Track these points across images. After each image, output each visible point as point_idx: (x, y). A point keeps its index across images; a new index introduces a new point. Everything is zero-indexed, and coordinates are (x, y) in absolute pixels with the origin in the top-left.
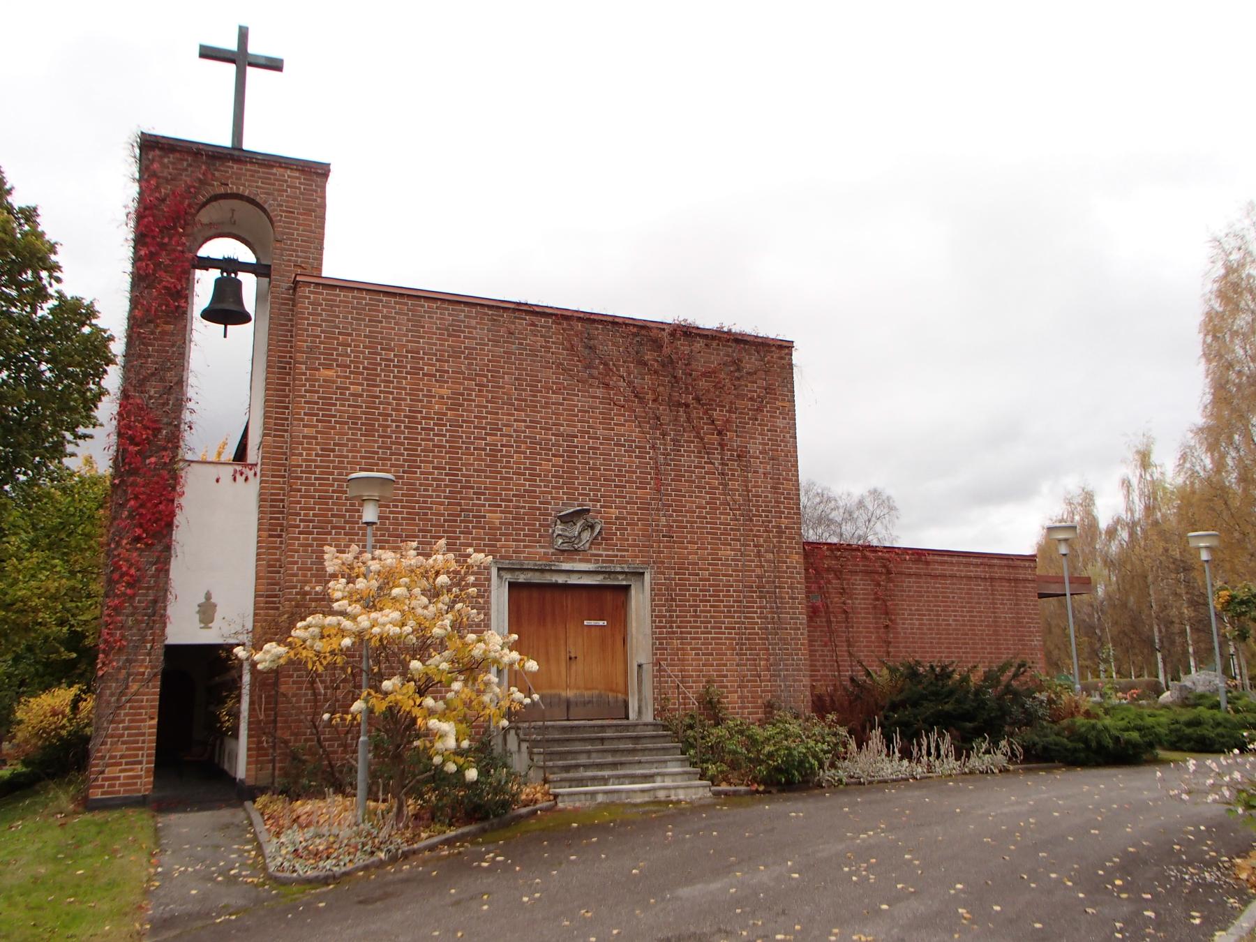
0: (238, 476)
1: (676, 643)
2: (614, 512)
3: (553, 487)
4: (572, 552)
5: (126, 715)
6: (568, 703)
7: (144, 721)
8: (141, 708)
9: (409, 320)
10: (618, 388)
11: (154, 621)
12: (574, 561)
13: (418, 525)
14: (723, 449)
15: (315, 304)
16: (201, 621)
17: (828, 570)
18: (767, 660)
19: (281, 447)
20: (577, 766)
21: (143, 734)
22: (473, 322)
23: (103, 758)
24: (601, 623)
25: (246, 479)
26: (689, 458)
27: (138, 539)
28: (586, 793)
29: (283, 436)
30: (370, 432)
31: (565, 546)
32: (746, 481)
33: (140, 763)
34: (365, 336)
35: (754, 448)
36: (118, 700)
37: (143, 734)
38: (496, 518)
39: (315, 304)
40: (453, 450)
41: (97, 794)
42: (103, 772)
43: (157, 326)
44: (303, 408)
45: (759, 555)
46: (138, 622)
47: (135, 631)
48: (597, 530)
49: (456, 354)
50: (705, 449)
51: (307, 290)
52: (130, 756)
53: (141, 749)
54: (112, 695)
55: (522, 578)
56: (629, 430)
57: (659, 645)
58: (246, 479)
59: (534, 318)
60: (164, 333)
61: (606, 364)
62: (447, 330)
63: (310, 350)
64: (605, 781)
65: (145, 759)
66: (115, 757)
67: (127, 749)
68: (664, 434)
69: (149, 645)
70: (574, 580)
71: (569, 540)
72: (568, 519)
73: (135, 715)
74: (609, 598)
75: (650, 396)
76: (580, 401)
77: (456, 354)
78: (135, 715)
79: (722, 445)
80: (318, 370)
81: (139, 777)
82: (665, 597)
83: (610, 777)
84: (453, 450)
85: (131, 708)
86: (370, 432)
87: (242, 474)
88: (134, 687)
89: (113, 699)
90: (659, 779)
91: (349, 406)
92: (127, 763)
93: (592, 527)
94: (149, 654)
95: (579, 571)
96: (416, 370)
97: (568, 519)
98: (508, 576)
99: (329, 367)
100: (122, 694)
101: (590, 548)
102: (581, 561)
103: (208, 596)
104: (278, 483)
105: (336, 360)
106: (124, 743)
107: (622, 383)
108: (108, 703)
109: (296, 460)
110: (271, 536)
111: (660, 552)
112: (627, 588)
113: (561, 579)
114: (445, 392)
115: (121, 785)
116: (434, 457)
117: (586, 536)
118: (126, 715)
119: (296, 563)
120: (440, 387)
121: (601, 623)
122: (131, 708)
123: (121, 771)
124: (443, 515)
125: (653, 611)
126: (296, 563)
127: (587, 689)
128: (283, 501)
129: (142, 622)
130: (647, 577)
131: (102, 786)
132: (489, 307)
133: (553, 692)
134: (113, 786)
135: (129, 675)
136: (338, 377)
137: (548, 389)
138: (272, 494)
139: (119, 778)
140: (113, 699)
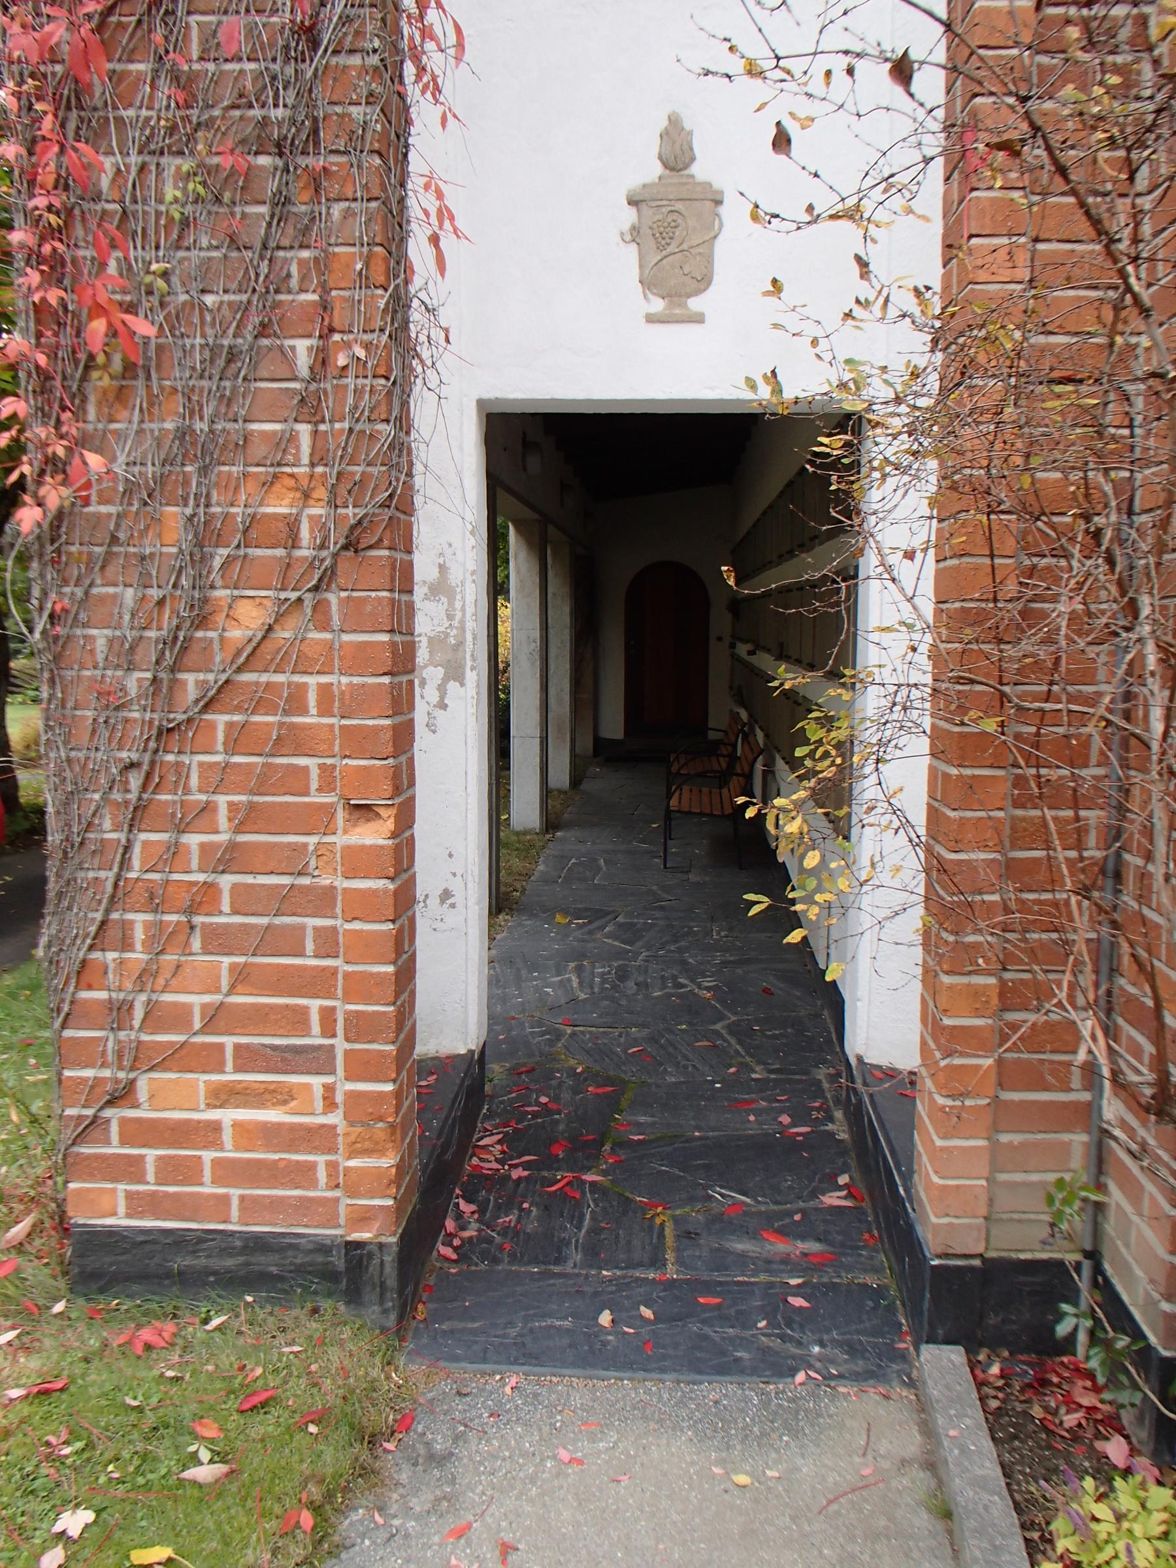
5: (220, 778)
7: (320, 819)
8: (293, 740)
11: (316, 181)
16: (649, 284)
21: (323, 901)
23: (119, 1013)
36: (161, 689)
37: (323, 901)
42: (123, 1095)
46: (220, 189)
47: (205, 246)
52: (259, 1018)
53: (320, 983)
66: (179, 1018)
67: (241, 978)
69: (302, 349)
73: (264, 781)
78: (264, 781)
81: (320, 1138)
85: (237, 740)
88: (245, 617)
92: (247, 1058)
94: (309, 407)
100: (179, 651)
103: (677, 153)
106: (218, 940)
108: (112, 702)
115: (227, 1172)
118: (220, 778)
122: (237, 740)
123: (223, 1096)
129: (246, 183)
131: (131, 1169)
134: (188, 1171)
135: (205, 535)
140: (135, 682)
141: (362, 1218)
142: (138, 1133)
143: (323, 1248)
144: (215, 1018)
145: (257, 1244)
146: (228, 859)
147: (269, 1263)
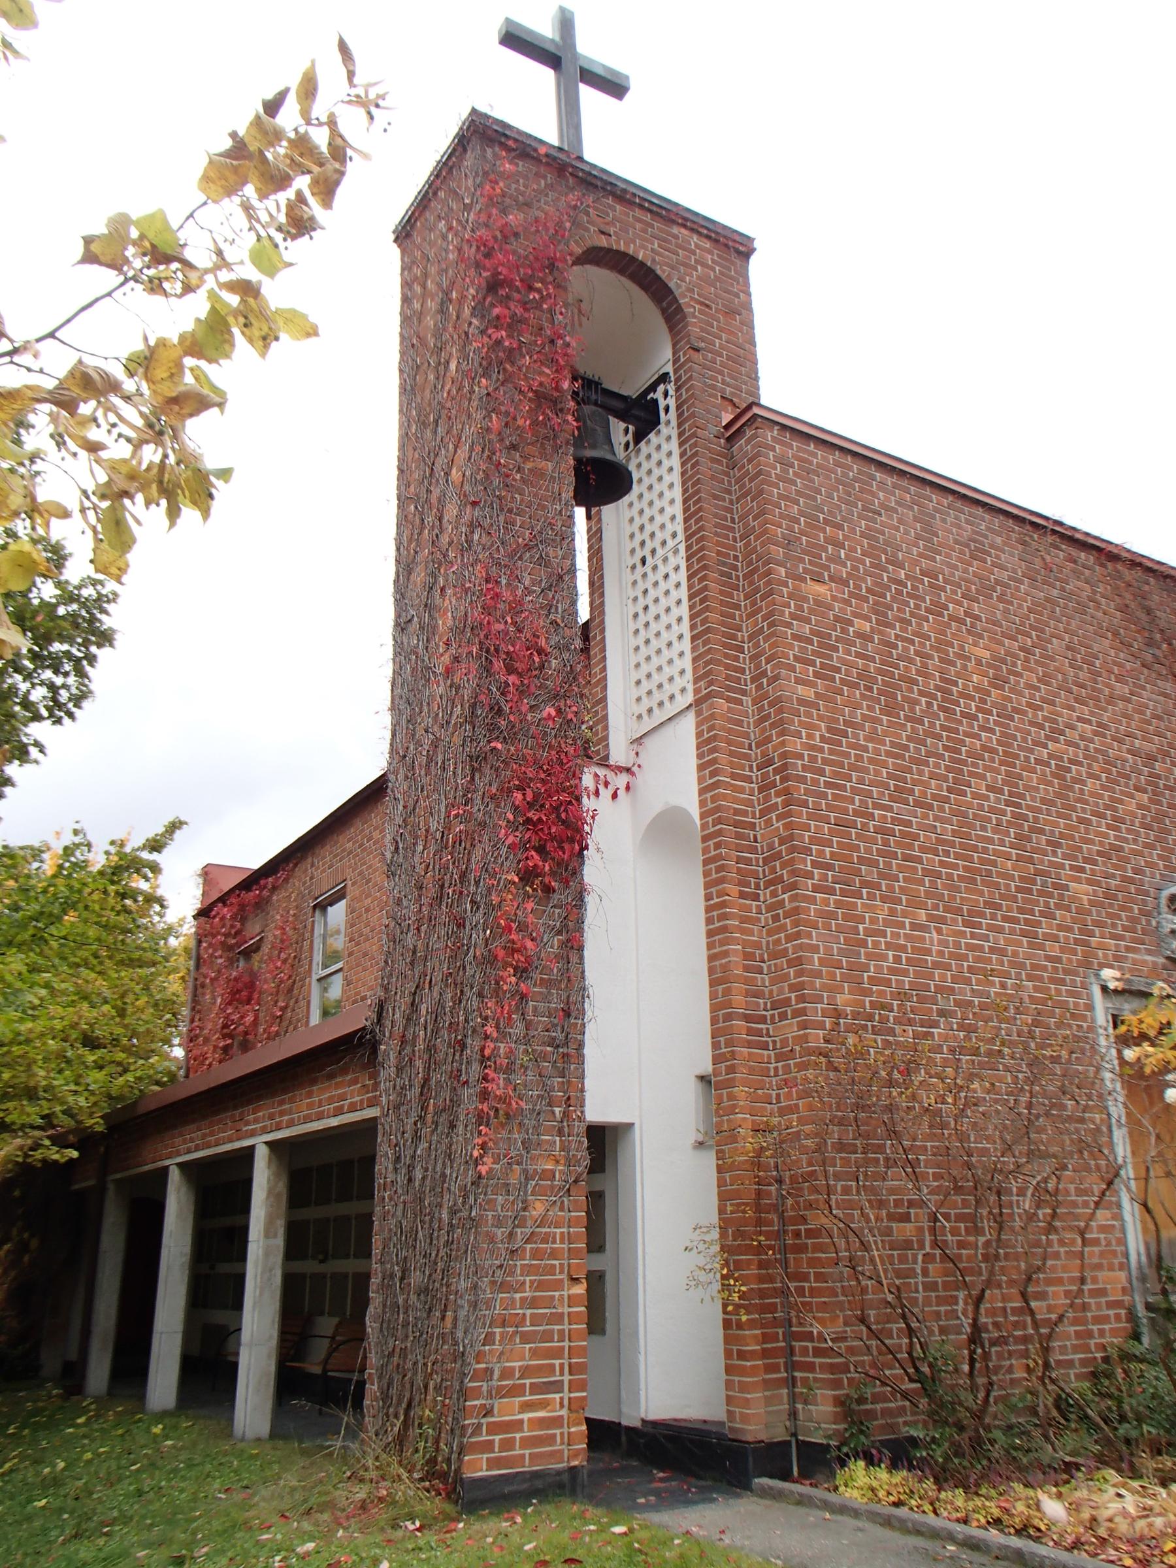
0: (601, 787)
3: (1146, 846)
5: (528, 1270)
7: (558, 1286)
8: (554, 1254)
9: (916, 519)
13: (982, 894)
19: (739, 723)
21: (558, 1318)
22: (999, 540)
23: (488, 1373)
25: (615, 796)
29: (740, 702)
30: (891, 709)
33: (557, 1387)
34: (863, 535)
37: (558, 1318)
40: (1009, 759)
41: (478, 1467)
42: (489, 1413)
43: (526, 458)
44: (792, 647)
52: (538, 1371)
53: (557, 1353)
54: (499, 1223)
58: (615, 796)
59: (1074, 552)
60: (538, 473)
62: (968, 546)
65: (566, 1378)
67: (535, 1353)
77: (986, 590)
80: (804, 580)
81: (556, 1422)
85: (536, 1254)
87: (606, 784)
88: (538, 1209)
89: (500, 1233)
91: (858, 655)
92: (535, 1389)
96: (938, 609)
99: (819, 581)
104: (741, 790)
105: (828, 568)
106: (526, 1338)
108: (492, 1239)
110: (742, 895)
115: (527, 1442)
116: (986, 768)
119: (815, 949)
120: (975, 644)
122: (536, 1254)
123: (527, 1407)
124: (1012, 878)
126: (815, 949)
128: (752, 826)
131: (488, 1446)
134: (507, 1445)
136: (834, 598)
138: (737, 812)
139: (517, 1425)
141: (576, 1454)
142: (494, 1428)
143: (559, 1473)
144: (526, 1372)
145: (535, 1475)
146: (533, 1303)
147: (539, 1484)
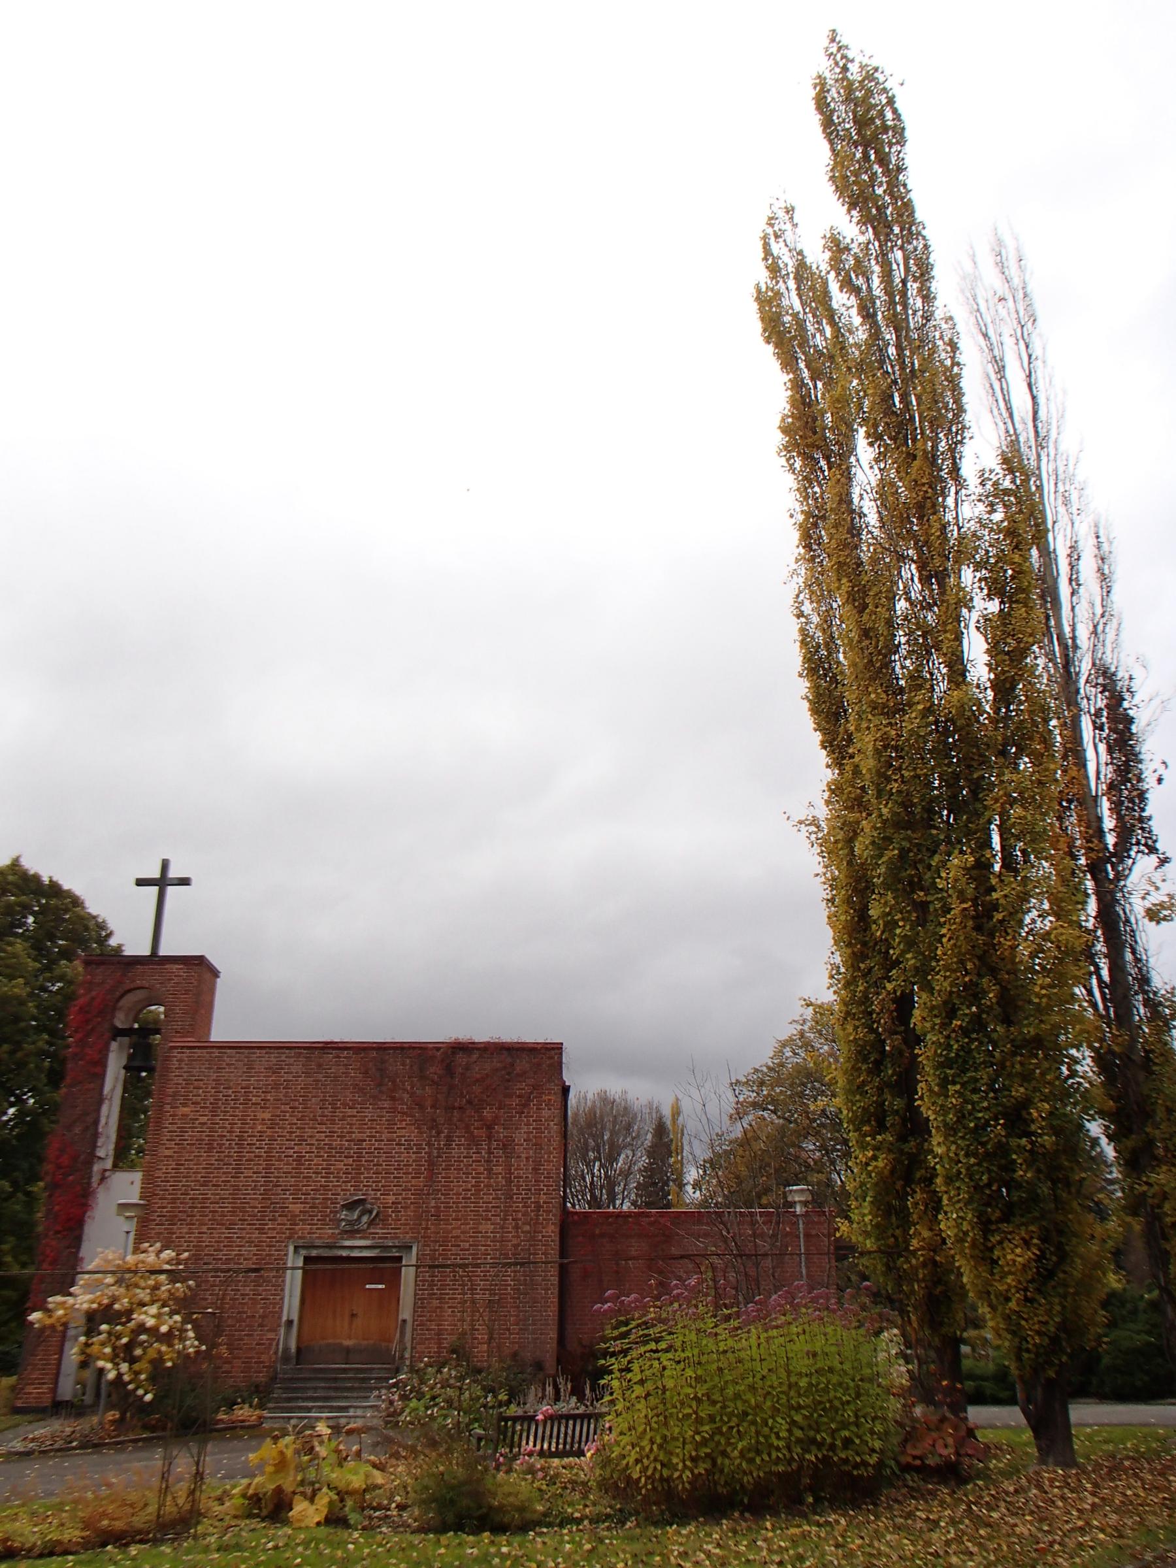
1: (436, 1303)
2: (391, 1199)
4: (352, 1233)
6: (348, 1350)
10: (401, 1099)
12: (355, 1238)
14: (490, 1141)
15: (180, 1061)
17: (602, 1235)
18: (517, 1316)
20: (298, 1398)
24: (380, 1286)
26: (458, 1150)
27: (57, 1232)
28: (283, 1418)
31: (348, 1228)
32: (508, 1166)
35: (520, 1137)
38: (296, 1208)
39: (180, 1061)
45: (517, 1227)
48: (374, 1213)
49: (276, 1086)
50: (473, 1141)
51: (175, 1053)
55: (314, 1253)
56: (408, 1132)
57: (419, 1304)
61: (394, 1082)
63: (175, 1094)
64: (309, 1410)
68: (439, 1133)
70: (356, 1254)
71: (350, 1223)
72: (351, 1206)
74: (385, 1267)
75: (429, 1103)
76: (369, 1113)
79: (489, 1137)
82: (429, 1266)
83: (313, 1407)
84: (269, 1158)
86: (210, 1149)
90: (352, 1410)
93: (370, 1212)
95: (359, 1246)
97: (351, 1206)
98: (303, 1252)
99: (184, 1105)
101: (368, 1228)
102: (361, 1238)
107: (406, 1096)
109: (158, 1174)
111: (427, 1228)
112: (400, 1259)
113: (344, 1253)
114: (267, 1116)
117: (365, 1219)
121: (380, 1286)
125: (417, 1276)
127: (364, 1339)
130: (414, 1250)
132: (305, 1048)
133: (338, 1341)
137: (345, 1105)
